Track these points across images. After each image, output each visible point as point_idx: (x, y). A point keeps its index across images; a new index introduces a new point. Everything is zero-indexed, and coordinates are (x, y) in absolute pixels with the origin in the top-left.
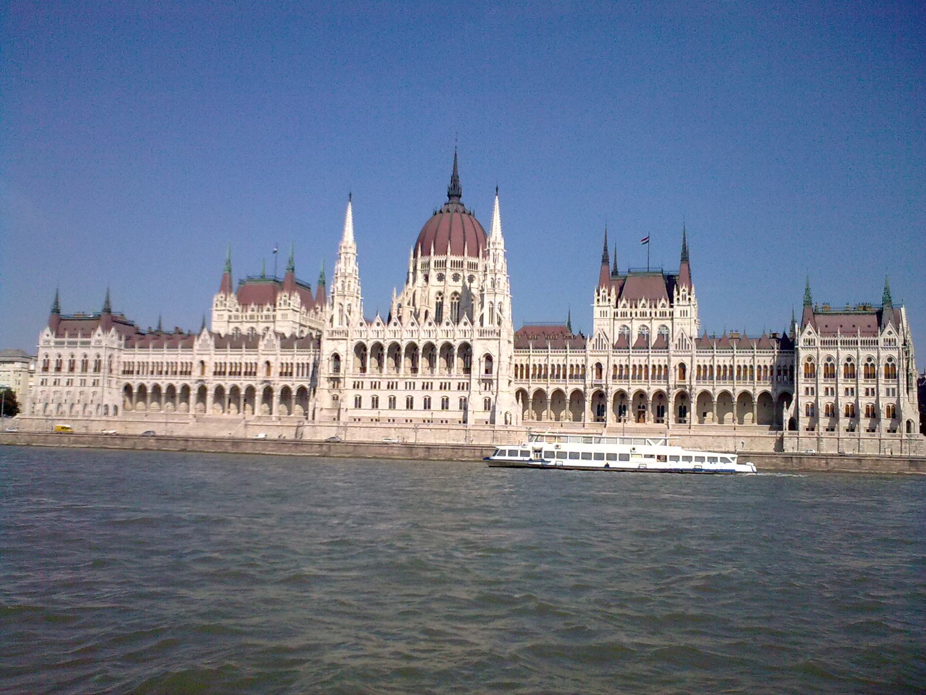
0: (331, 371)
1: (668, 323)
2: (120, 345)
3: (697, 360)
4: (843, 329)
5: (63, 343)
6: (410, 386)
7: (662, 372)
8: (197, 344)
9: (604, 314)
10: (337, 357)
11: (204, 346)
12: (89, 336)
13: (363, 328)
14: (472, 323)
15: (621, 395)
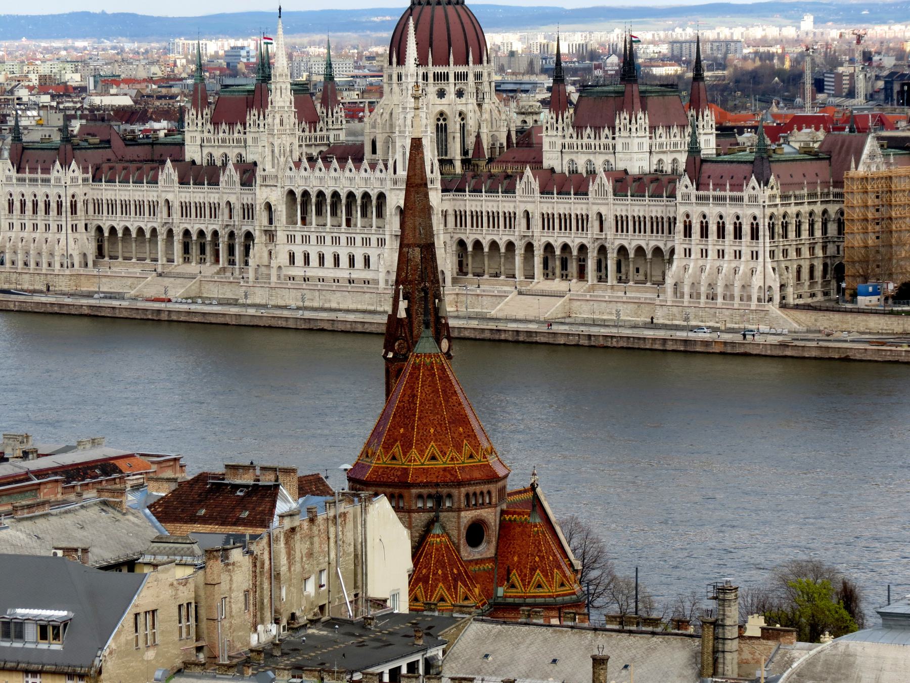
0: (265, 222)
1: (611, 158)
2: (85, 180)
3: (612, 208)
4: (721, 182)
5: (24, 180)
6: (336, 241)
7: (582, 221)
8: (161, 177)
9: (552, 144)
10: (269, 207)
11: (169, 180)
12: (46, 170)
13: (291, 174)
14: (387, 169)
15: (549, 247)
